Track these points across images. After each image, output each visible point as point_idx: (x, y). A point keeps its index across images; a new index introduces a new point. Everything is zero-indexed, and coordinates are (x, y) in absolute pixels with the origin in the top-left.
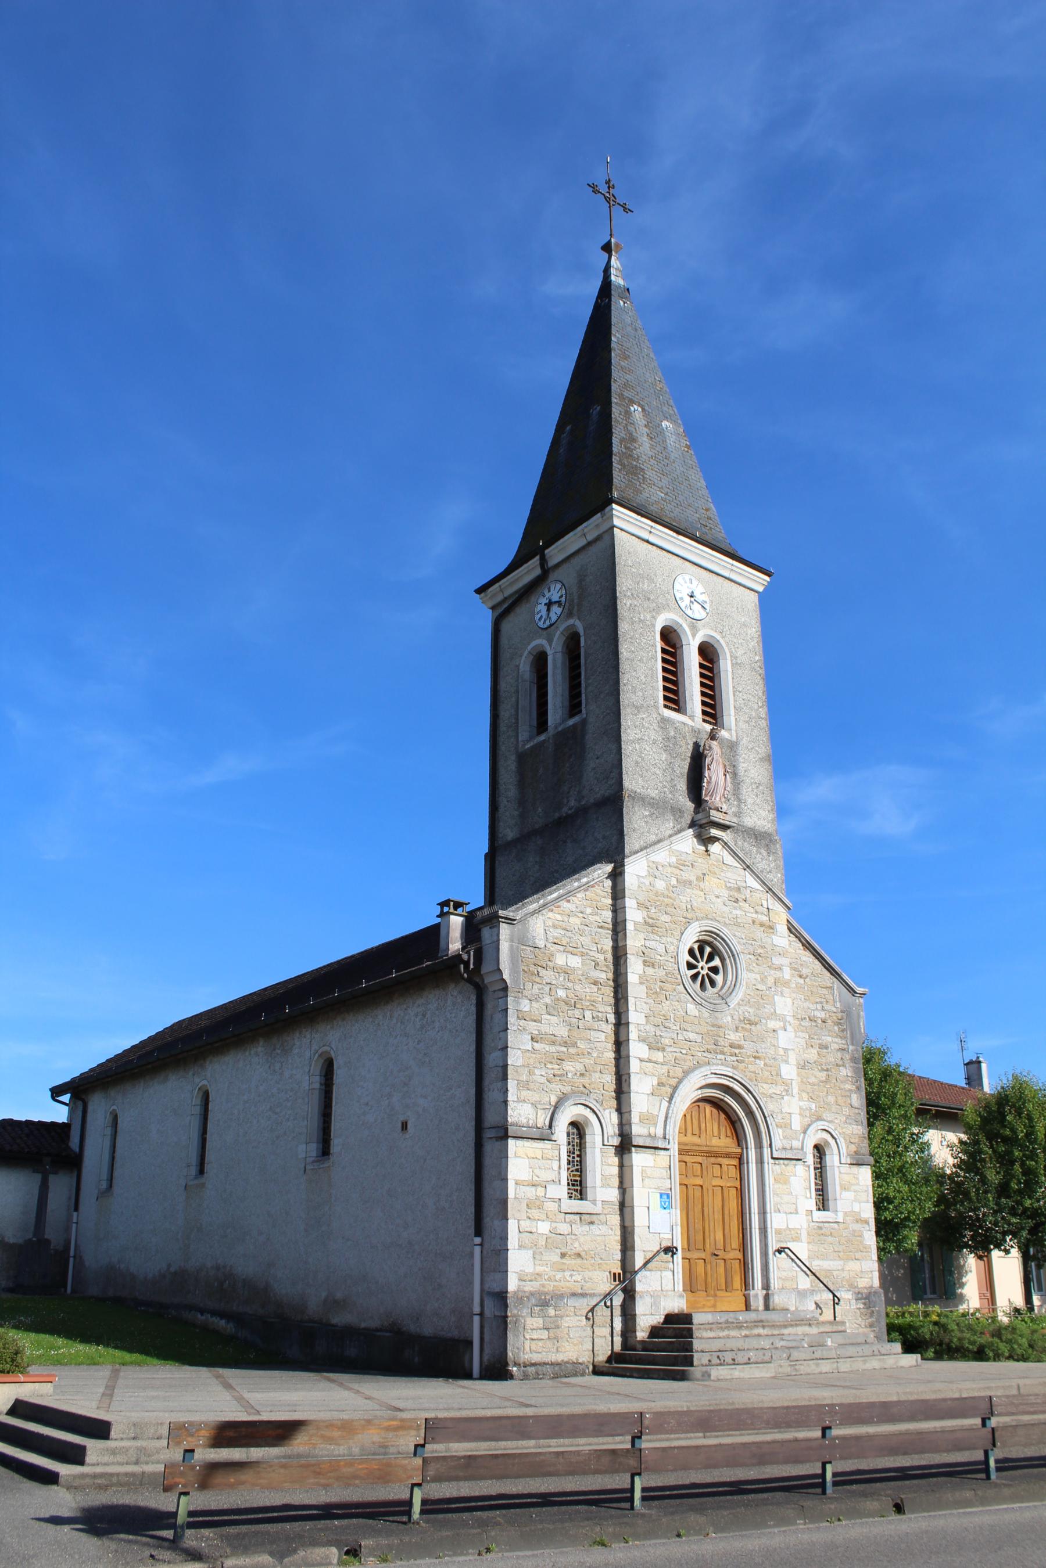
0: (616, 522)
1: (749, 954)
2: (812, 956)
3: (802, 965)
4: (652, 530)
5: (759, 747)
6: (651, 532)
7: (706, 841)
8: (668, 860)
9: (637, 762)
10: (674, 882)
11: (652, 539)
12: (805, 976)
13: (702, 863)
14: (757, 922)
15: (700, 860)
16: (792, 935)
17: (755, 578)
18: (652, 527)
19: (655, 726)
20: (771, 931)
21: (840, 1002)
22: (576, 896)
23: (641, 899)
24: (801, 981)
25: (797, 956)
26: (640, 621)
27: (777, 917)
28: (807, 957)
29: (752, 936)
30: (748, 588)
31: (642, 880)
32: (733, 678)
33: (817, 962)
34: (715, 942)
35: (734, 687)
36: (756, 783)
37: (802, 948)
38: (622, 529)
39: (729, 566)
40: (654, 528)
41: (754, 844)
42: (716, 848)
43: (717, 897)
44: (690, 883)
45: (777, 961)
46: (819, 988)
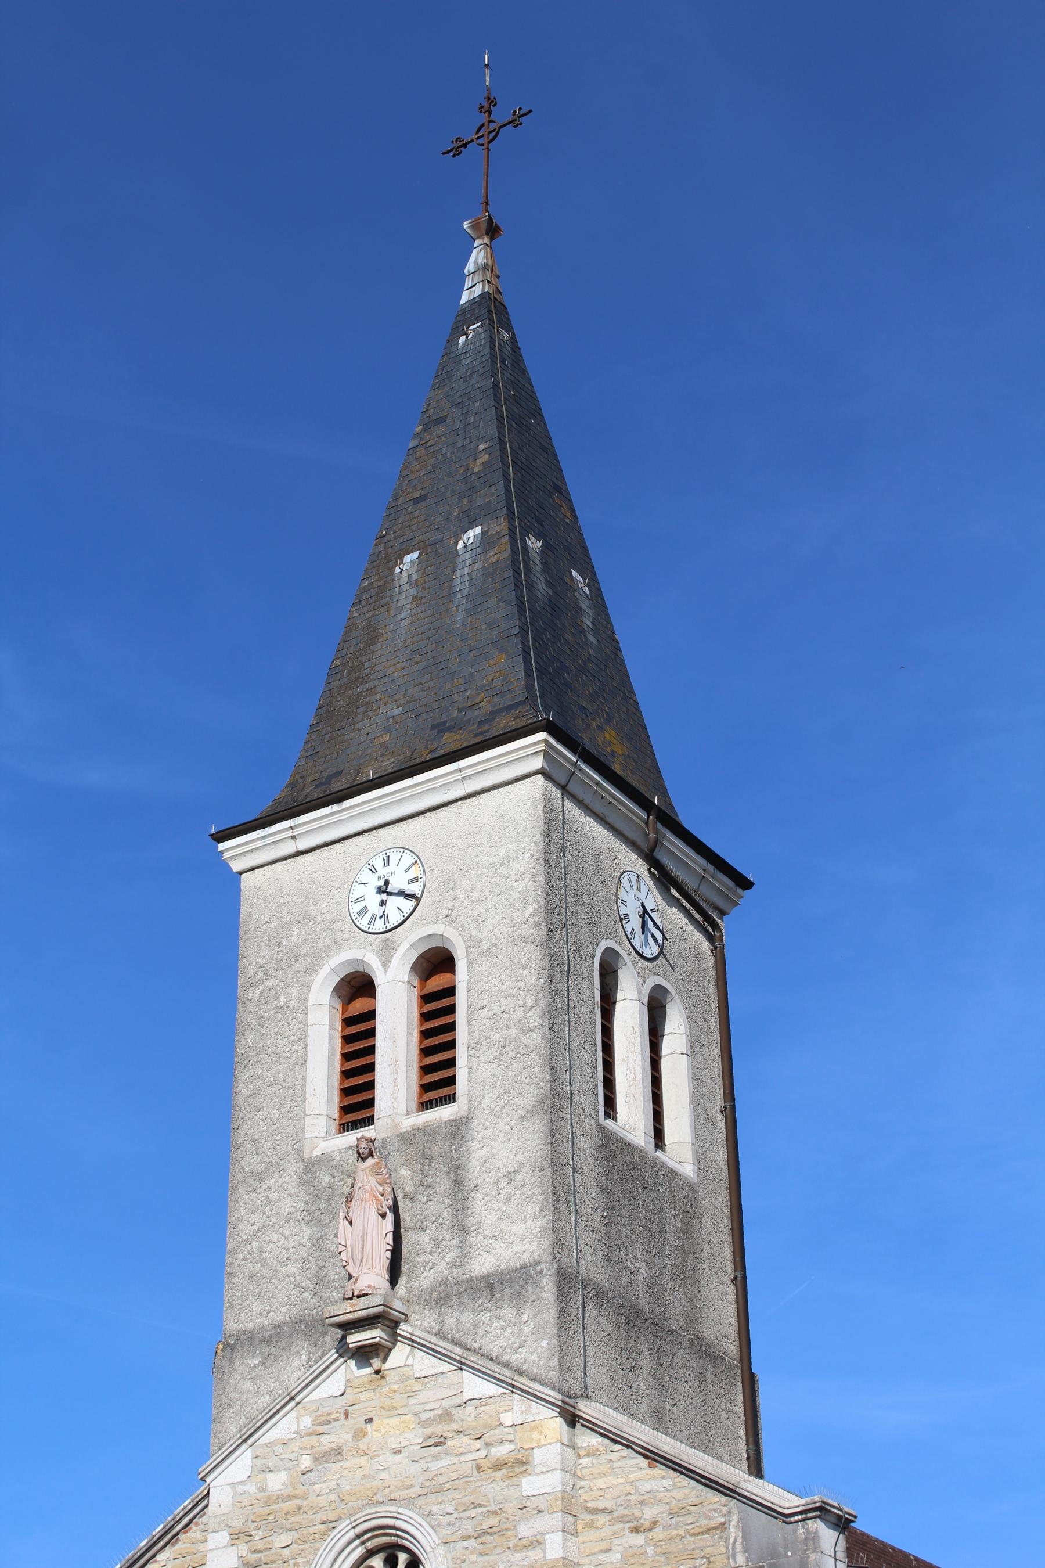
0: (236, 866)
1: (466, 1538)
2: (671, 1472)
3: (641, 1503)
4: (296, 832)
5: (521, 1095)
6: (293, 837)
7: (364, 1354)
8: (294, 1428)
9: (252, 1275)
10: (306, 1462)
11: (303, 845)
12: (647, 1524)
13: (369, 1400)
14: (485, 1464)
15: (363, 1397)
16: (618, 1447)
17: (516, 756)
18: (292, 828)
19: (293, 1188)
20: (524, 1468)
21: (746, 1550)
22: (155, 1561)
23: (237, 1524)
24: (640, 1539)
25: (629, 1489)
26: (279, 1009)
27: (535, 1435)
28: (662, 1480)
29: (471, 1499)
30: (517, 780)
31: (240, 1488)
32: (469, 990)
33: (683, 1481)
34: (400, 1542)
35: (469, 1007)
36: (509, 1173)
37: (644, 1463)
38: (253, 869)
39: (458, 776)
40: (297, 826)
41: (485, 1305)
42: (399, 1355)
43: (398, 1452)
44: (338, 1452)
45: (525, 1530)
46: (689, 1538)
